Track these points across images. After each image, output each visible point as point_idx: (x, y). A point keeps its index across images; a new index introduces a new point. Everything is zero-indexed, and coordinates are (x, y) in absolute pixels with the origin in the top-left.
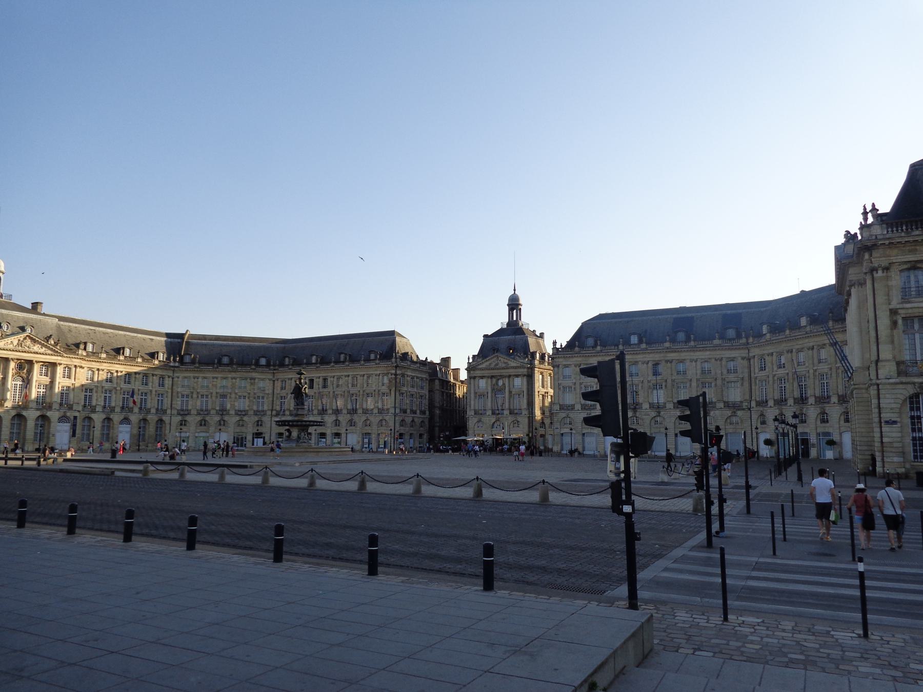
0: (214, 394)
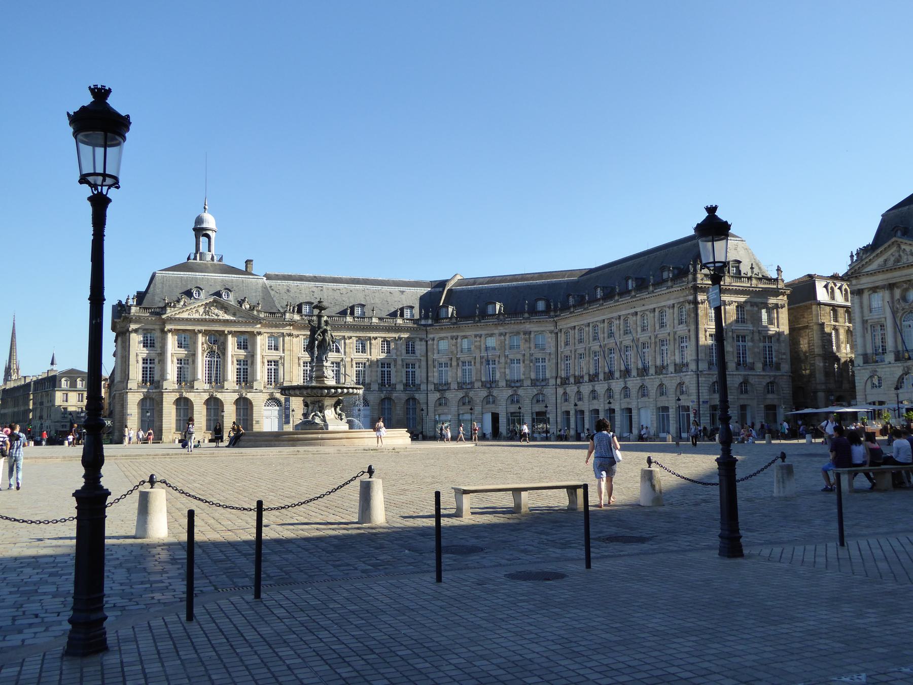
0: (478, 360)
